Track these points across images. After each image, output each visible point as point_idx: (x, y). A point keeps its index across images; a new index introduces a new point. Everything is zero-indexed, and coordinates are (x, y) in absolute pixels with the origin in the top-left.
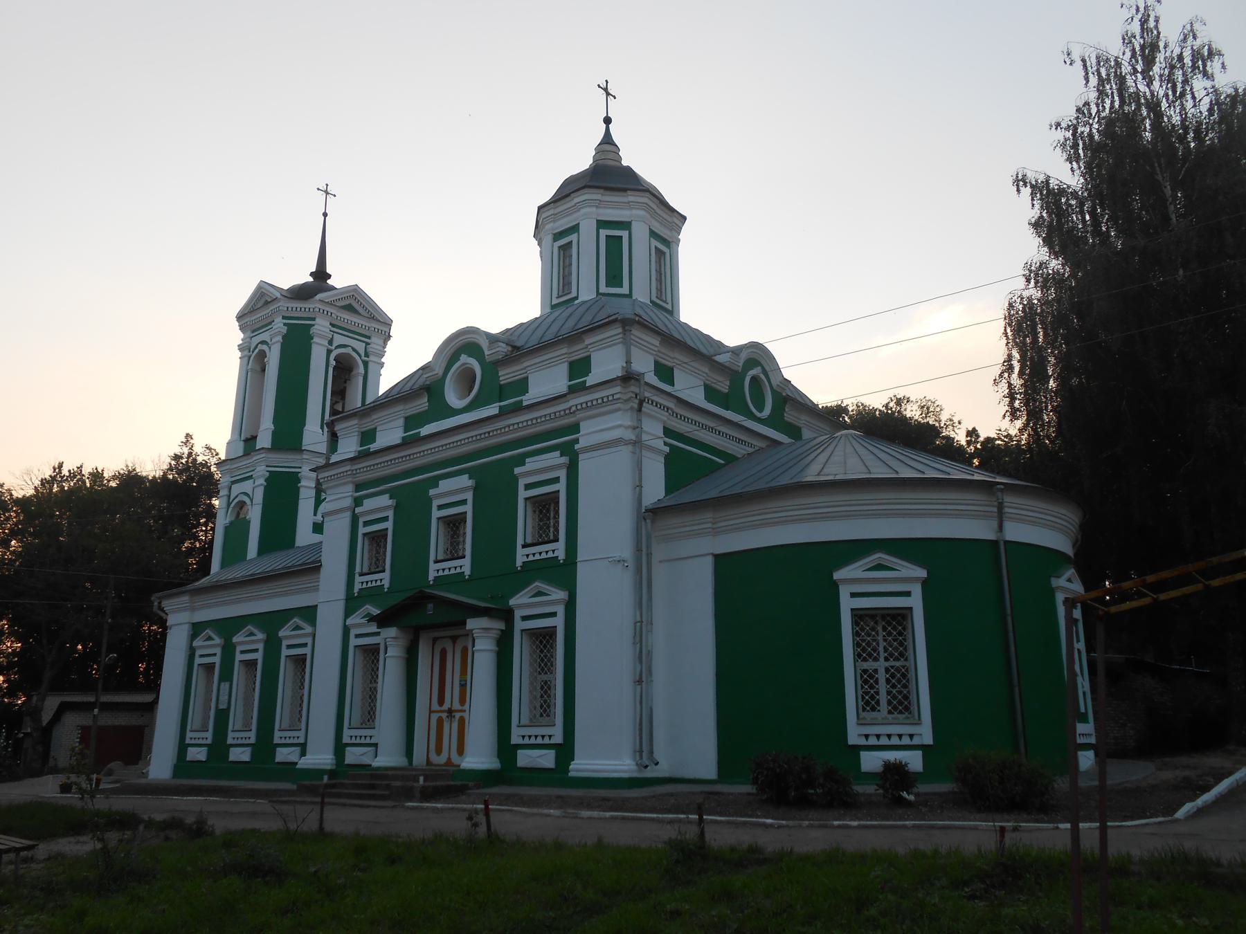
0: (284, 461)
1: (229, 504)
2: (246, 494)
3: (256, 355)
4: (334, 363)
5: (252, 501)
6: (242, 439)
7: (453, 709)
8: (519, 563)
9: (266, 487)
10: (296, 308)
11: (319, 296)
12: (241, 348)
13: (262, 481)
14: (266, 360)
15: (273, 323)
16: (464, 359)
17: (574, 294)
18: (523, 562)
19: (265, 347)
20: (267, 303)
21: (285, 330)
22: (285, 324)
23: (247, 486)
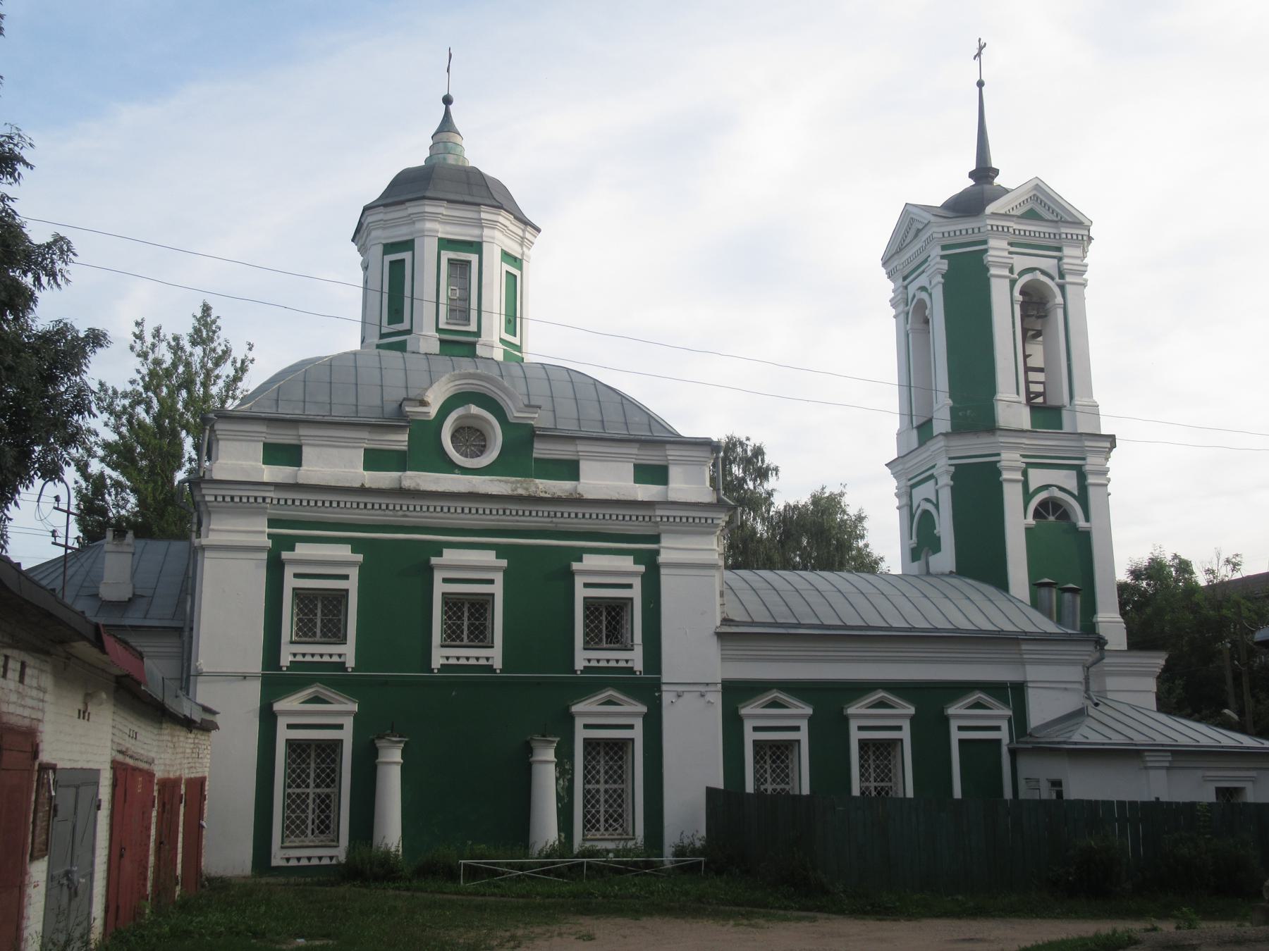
0: (973, 447)
1: (912, 516)
2: (927, 500)
3: (914, 307)
4: (1020, 298)
5: (937, 506)
6: (914, 425)
9: (952, 488)
10: (955, 232)
11: (990, 209)
12: (894, 303)
13: (945, 480)
14: (927, 312)
15: (929, 259)
19: (924, 295)
20: (919, 231)
21: (944, 266)
22: (943, 257)
23: (926, 490)
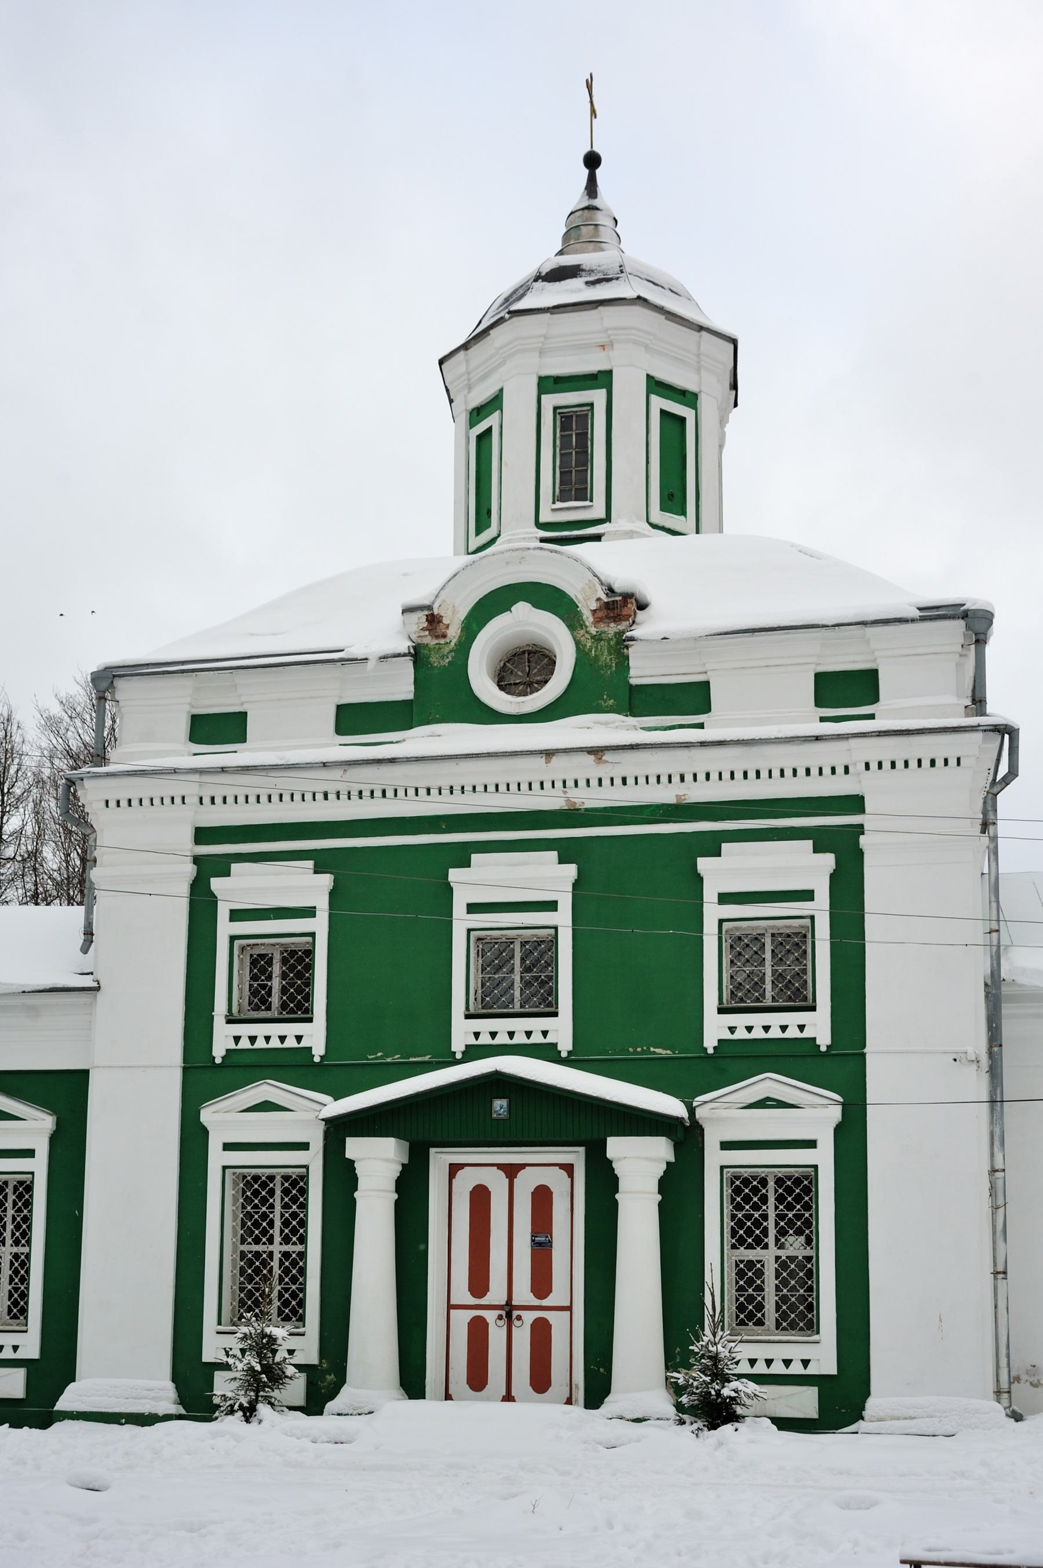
7: (514, 1303)
8: (710, 1043)
16: (522, 610)
17: (598, 510)
18: (719, 1041)
